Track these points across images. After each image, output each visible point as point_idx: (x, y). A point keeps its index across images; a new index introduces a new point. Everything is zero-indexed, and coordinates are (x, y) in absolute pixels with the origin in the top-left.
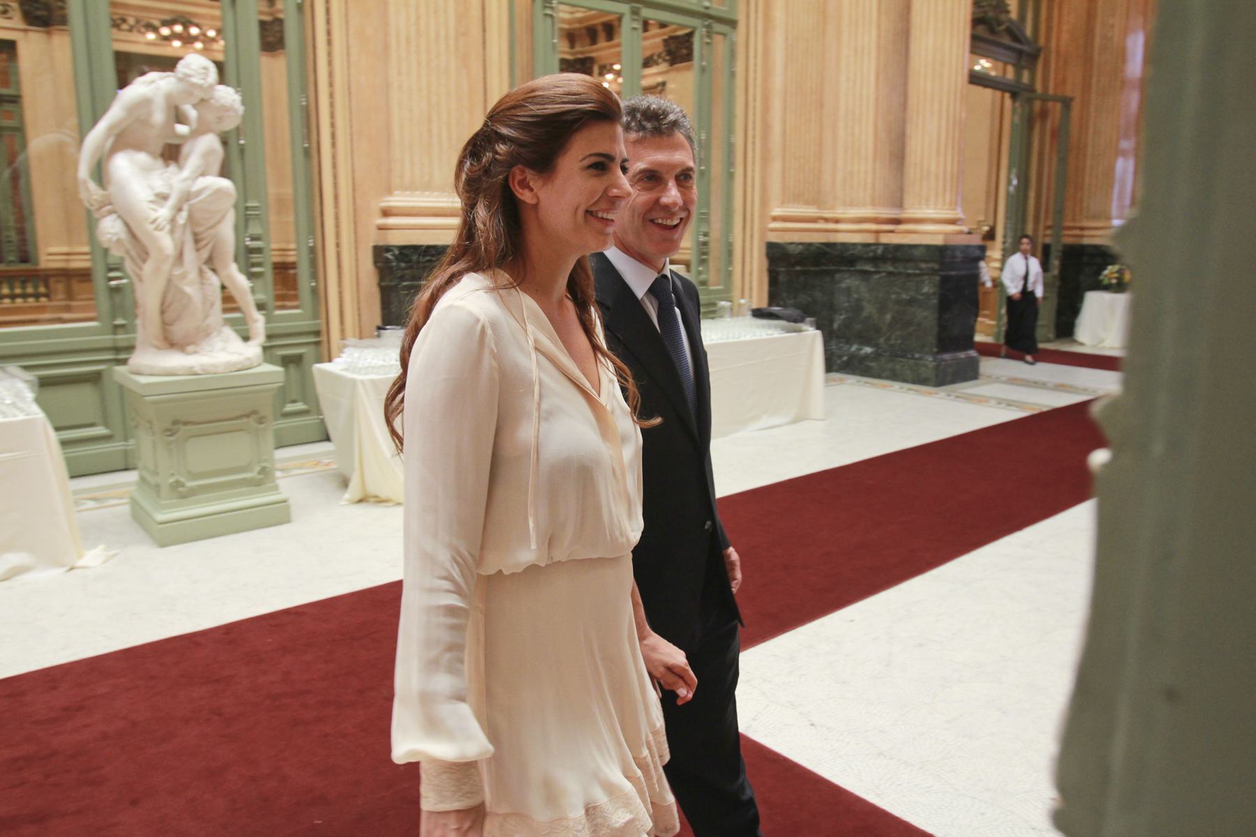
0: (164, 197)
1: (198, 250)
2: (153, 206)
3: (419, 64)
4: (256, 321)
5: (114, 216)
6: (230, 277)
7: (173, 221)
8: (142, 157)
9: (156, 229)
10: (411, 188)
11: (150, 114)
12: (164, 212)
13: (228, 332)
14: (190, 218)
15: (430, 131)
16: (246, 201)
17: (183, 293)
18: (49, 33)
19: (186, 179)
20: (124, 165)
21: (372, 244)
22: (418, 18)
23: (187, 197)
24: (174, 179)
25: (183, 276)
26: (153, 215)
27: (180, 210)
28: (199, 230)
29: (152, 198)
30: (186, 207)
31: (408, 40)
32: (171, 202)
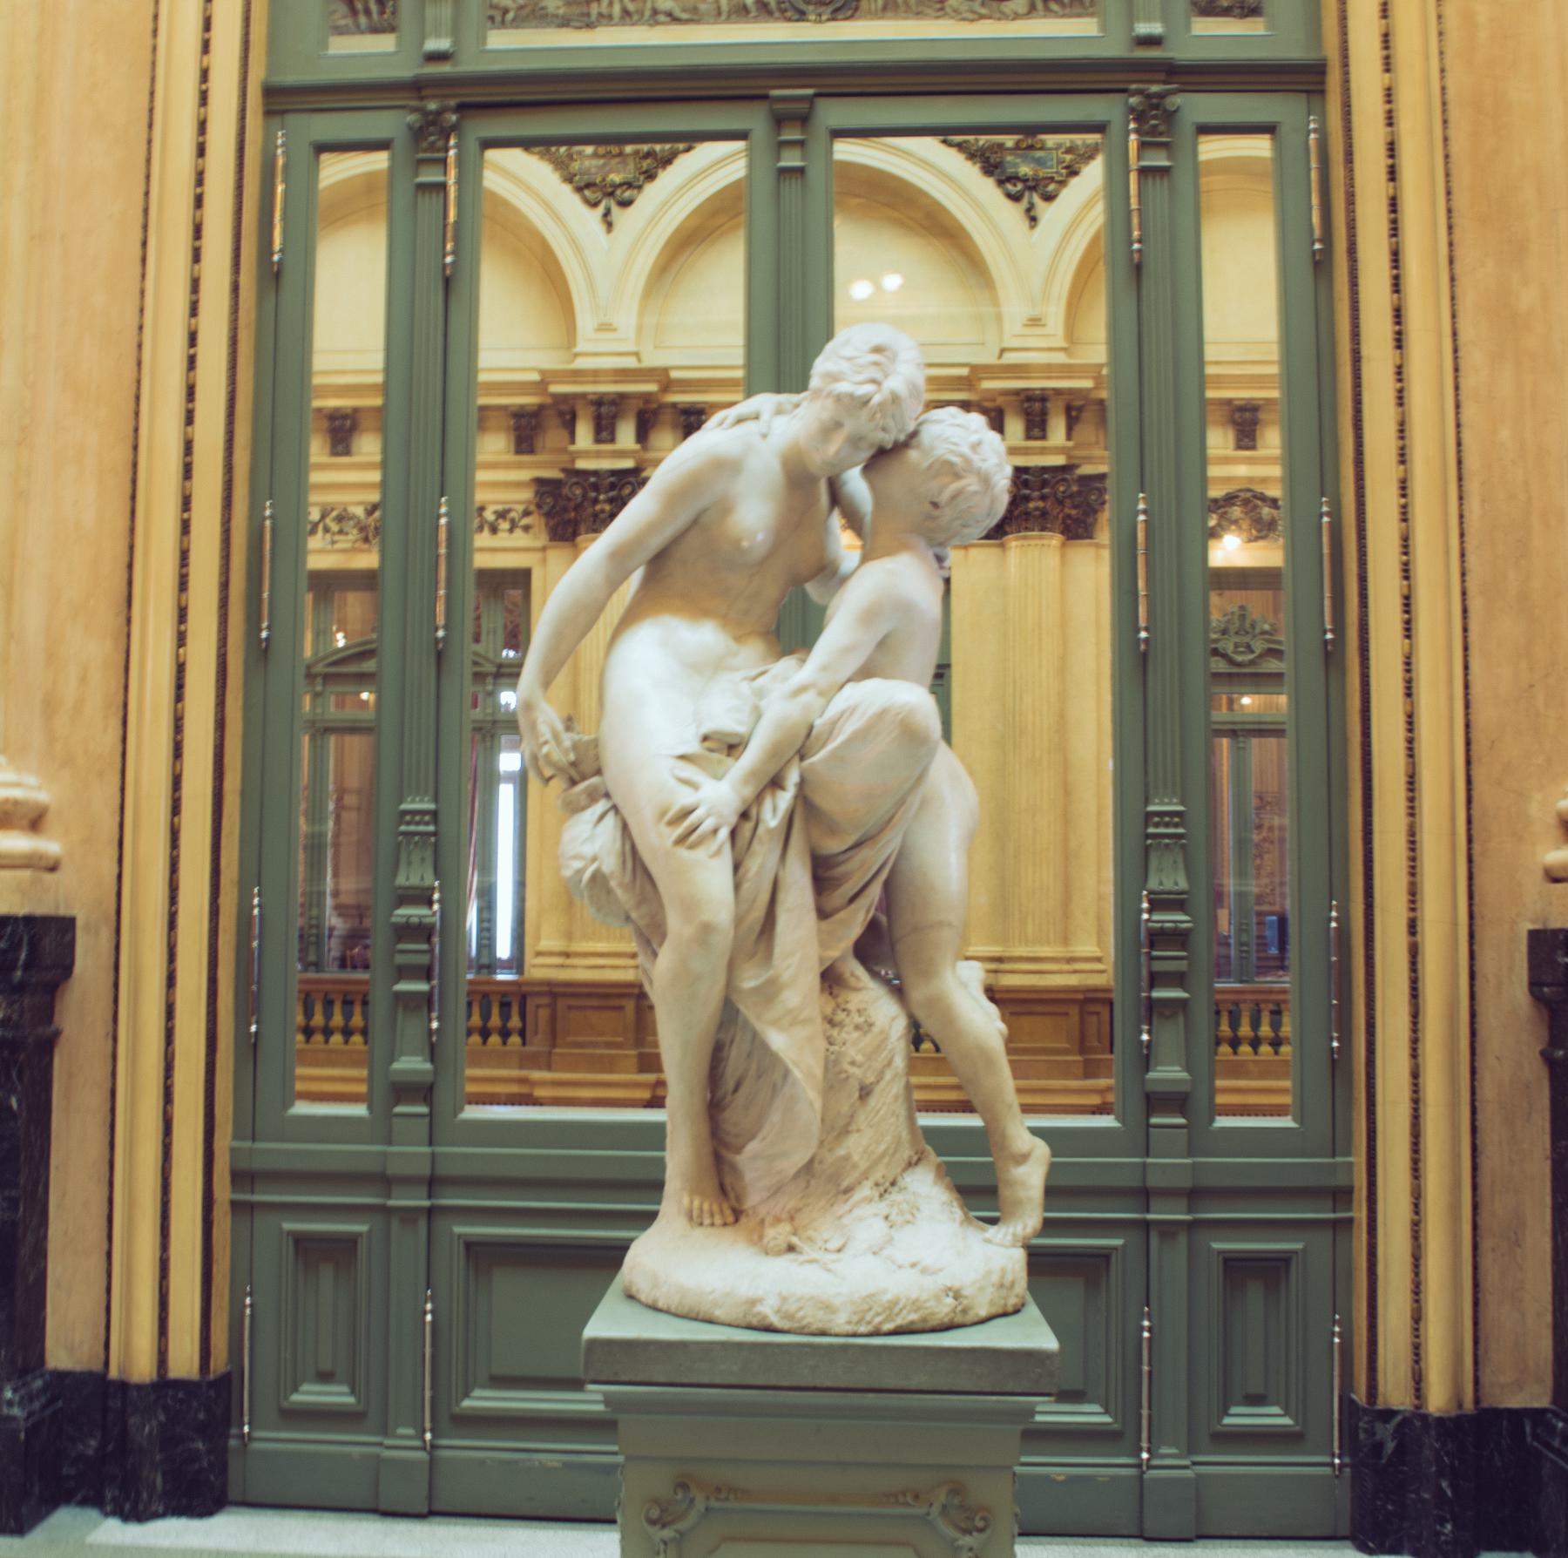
1: (823, 914)
2: (689, 771)
4: (1023, 1158)
5: (601, 806)
6: (940, 1005)
8: (704, 636)
9: (681, 840)
12: (719, 794)
13: (927, 1190)
14: (805, 803)
16: (1147, 801)
17: (765, 1048)
23: (802, 744)
24: (771, 695)
25: (769, 992)
27: (776, 783)
28: (832, 846)
30: (793, 778)
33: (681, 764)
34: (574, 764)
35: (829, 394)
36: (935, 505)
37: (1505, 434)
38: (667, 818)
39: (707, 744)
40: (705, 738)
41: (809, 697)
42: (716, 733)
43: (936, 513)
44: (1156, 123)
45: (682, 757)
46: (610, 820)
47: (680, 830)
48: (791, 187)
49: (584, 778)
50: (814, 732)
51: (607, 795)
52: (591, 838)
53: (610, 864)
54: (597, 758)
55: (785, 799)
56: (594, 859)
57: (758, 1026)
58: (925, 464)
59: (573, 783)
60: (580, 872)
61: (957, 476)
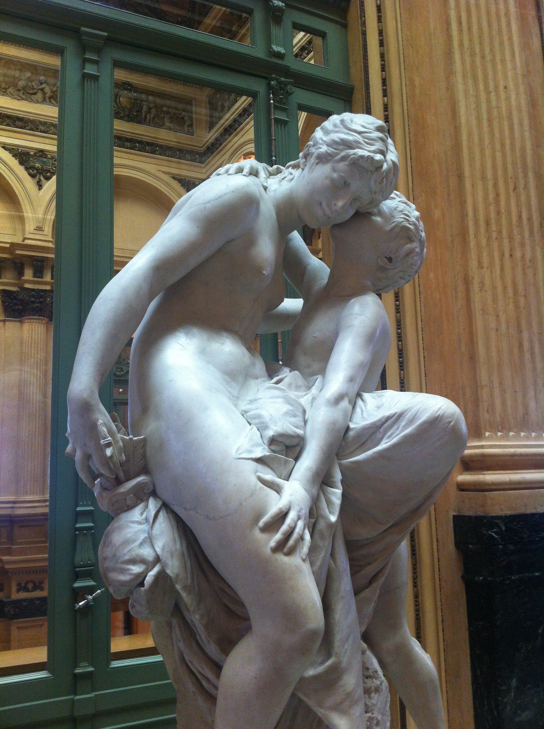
0: (287, 447)
3: (502, 255)
5: (152, 505)
7: (314, 515)
8: (228, 348)
10: (503, 427)
11: (250, 240)
15: (521, 345)
18: (21, 322)
19: (338, 399)
20: (188, 366)
21: (452, 513)
22: (498, 195)
26: (275, 504)
29: (261, 451)
31: (488, 223)
32: (308, 461)
33: (259, 467)
34: (122, 465)
35: (344, 159)
36: (390, 260)
37: (432, 275)
38: (261, 523)
39: (273, 447)
40: (273, 441)
41: (345, 404)
42: (282, 435)
43: (389, 266)
44: (281, 95)
45: (259, 460)
46: (162, 516)
47: (278, 536)
48: (88, 85)
49: (128, 479)
50: (351, 433)
51: (154, 494)
52: (150, 540)
53: (173, 567)
54: (144, 456)
55: (336, 494)
56: (158, 560)
57: (320, 712)
58: (388, 228)
59: (119, 482)
60: (143, 575)
61: (410, 240)
